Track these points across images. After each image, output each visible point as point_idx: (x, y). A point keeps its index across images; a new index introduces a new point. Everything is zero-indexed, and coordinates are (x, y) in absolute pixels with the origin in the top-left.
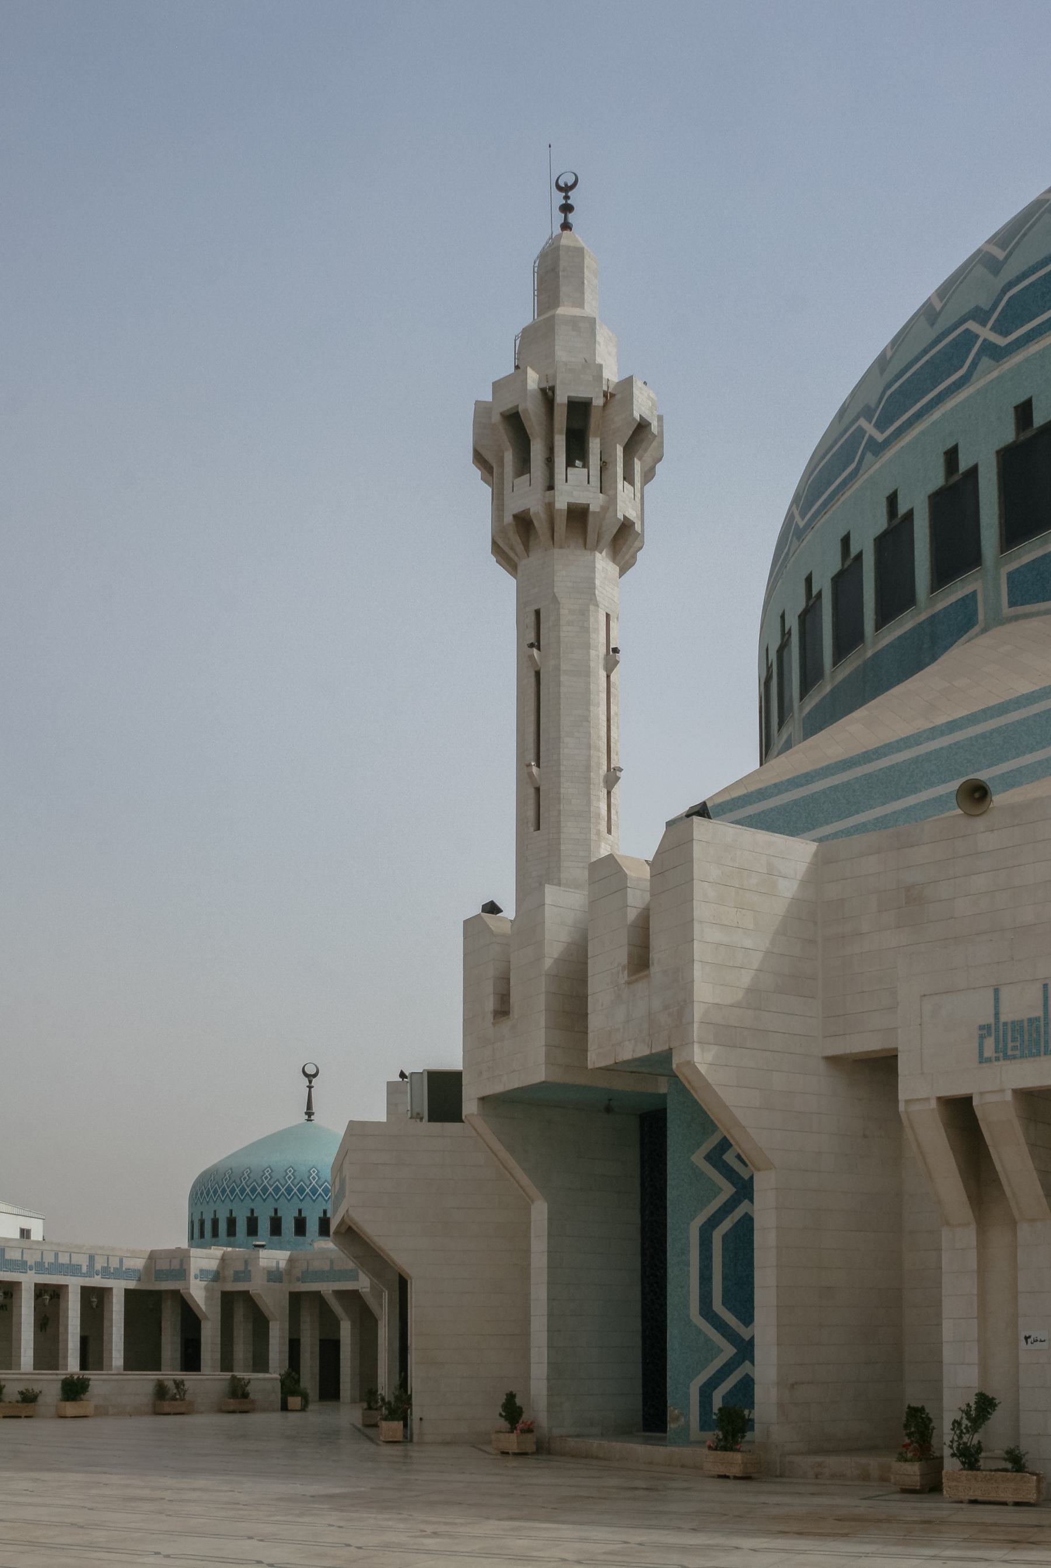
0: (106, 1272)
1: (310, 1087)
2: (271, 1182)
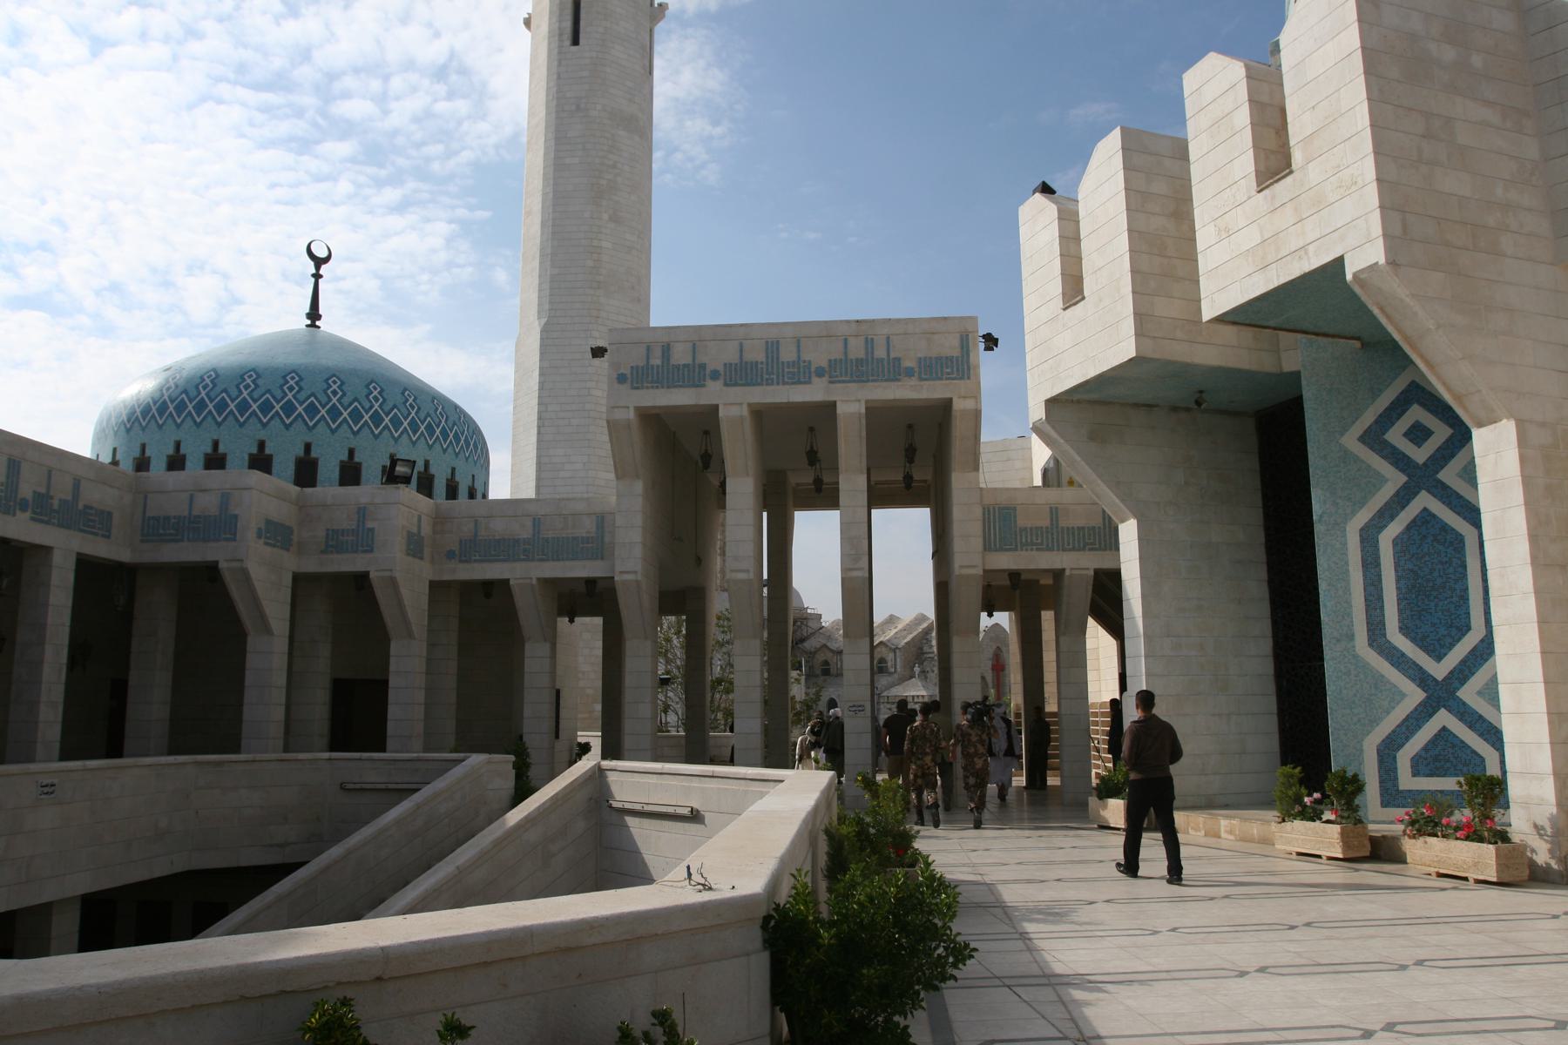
0: (42, 507)
1: (317, 276)
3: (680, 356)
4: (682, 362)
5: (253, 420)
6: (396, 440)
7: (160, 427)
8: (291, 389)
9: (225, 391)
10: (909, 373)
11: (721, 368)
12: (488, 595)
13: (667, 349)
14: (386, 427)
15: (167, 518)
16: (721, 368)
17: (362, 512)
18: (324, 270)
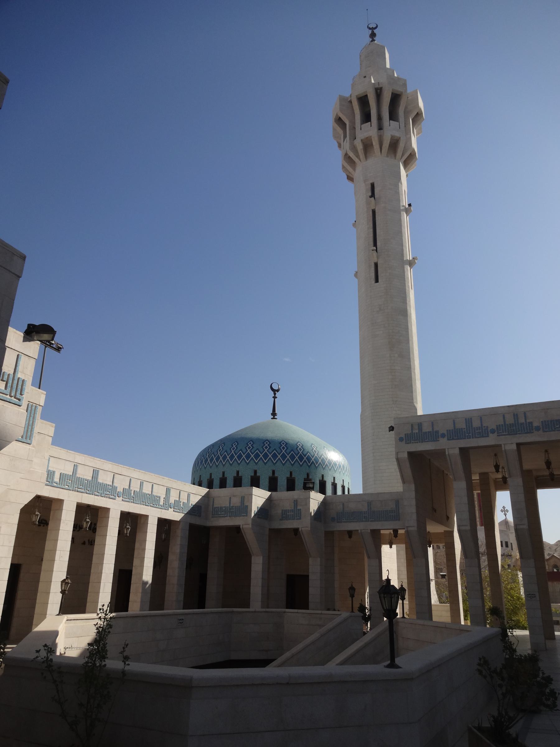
1: (275, 397)
2: (270, 451)
3: (426, 428)
4: (427, 431)
5: (252, 461)
6: (309, 467)
7: (217, 466)
8: (266, 447)
9: (241, 450)
10: (538, 429)
11: (445, 432)
12: (350, 537)
13: (420, 425)
14: (305, 461)
15: (221, 508)
16: (445, 432)
17: (296, 502)
18: (278, 394)
